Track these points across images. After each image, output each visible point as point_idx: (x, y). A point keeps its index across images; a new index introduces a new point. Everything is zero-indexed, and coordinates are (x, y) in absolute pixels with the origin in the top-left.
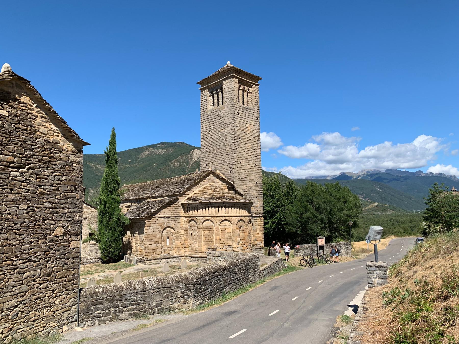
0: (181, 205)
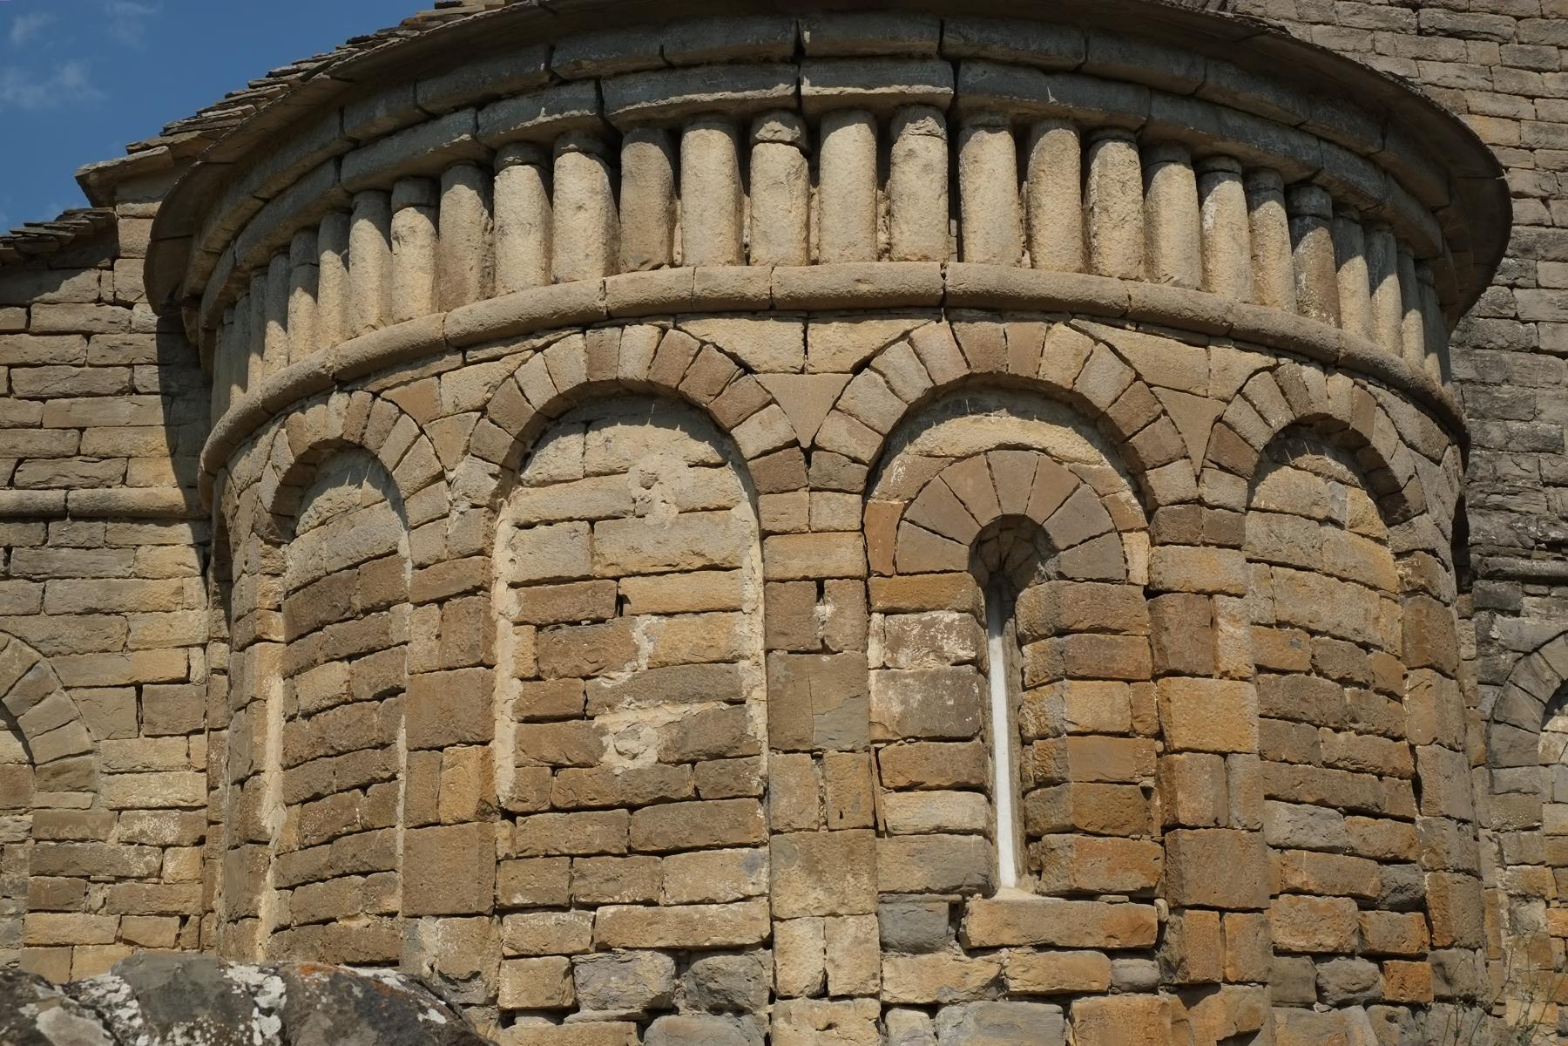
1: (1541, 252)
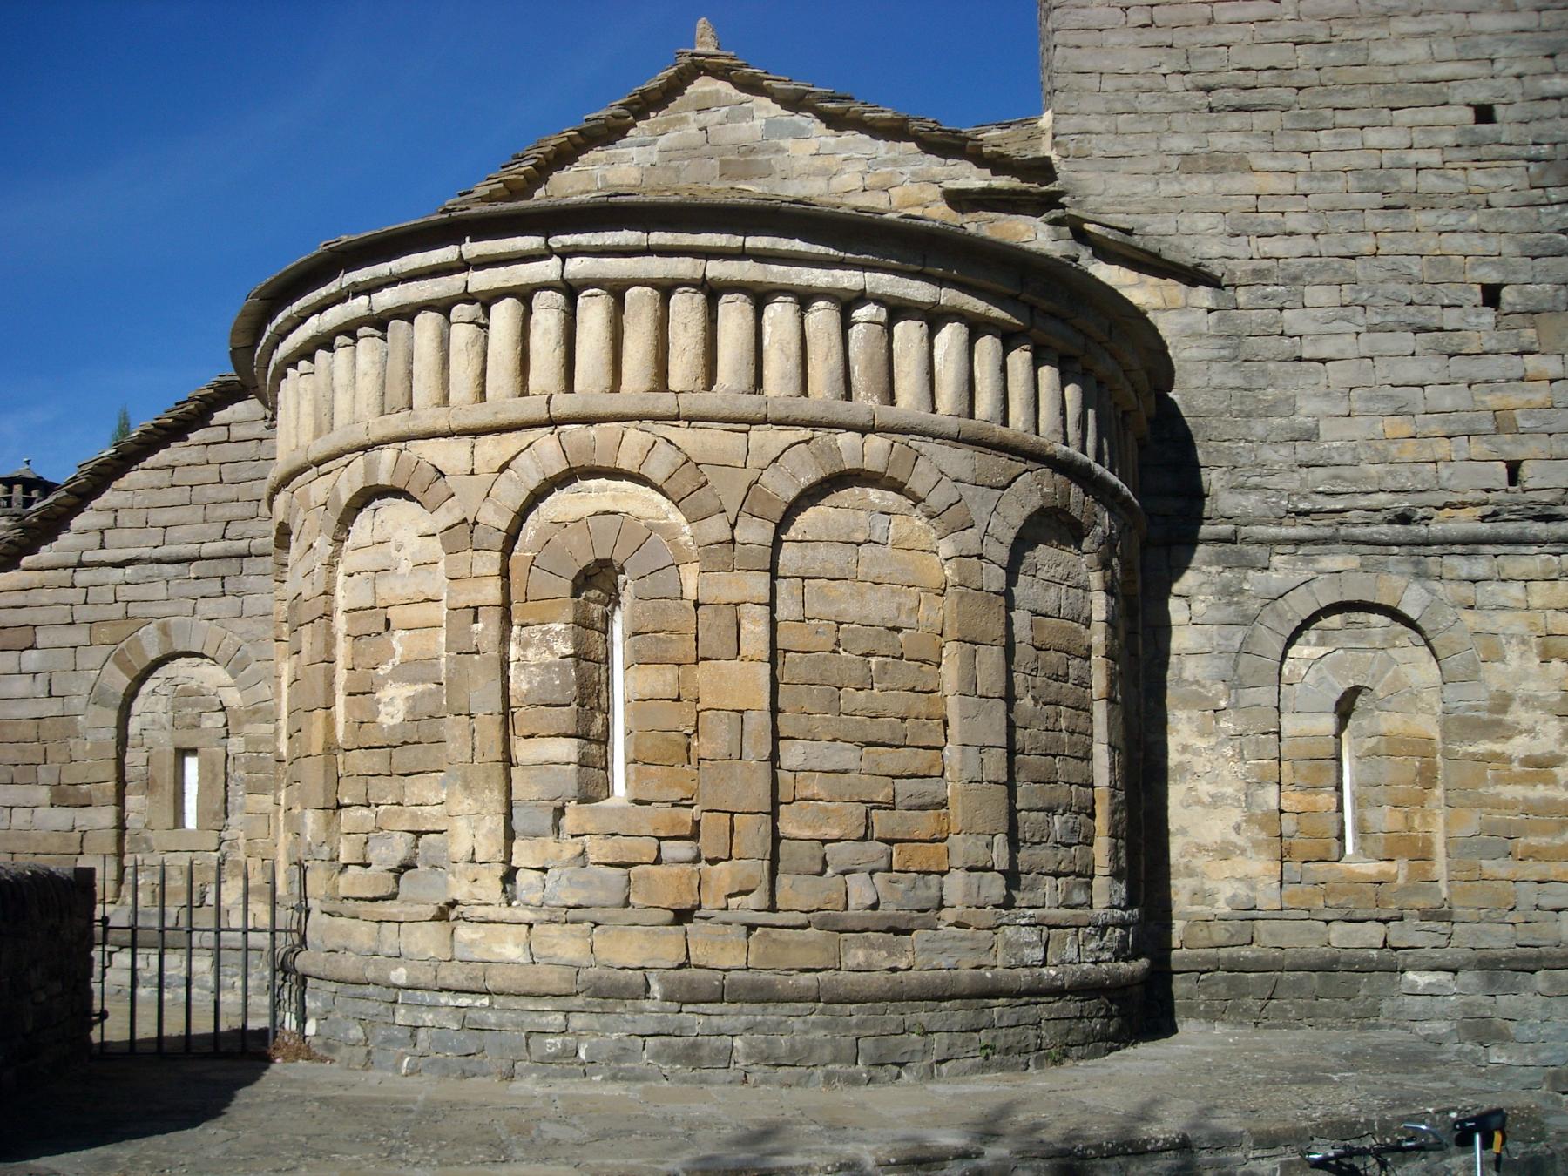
1: (1308, 278)
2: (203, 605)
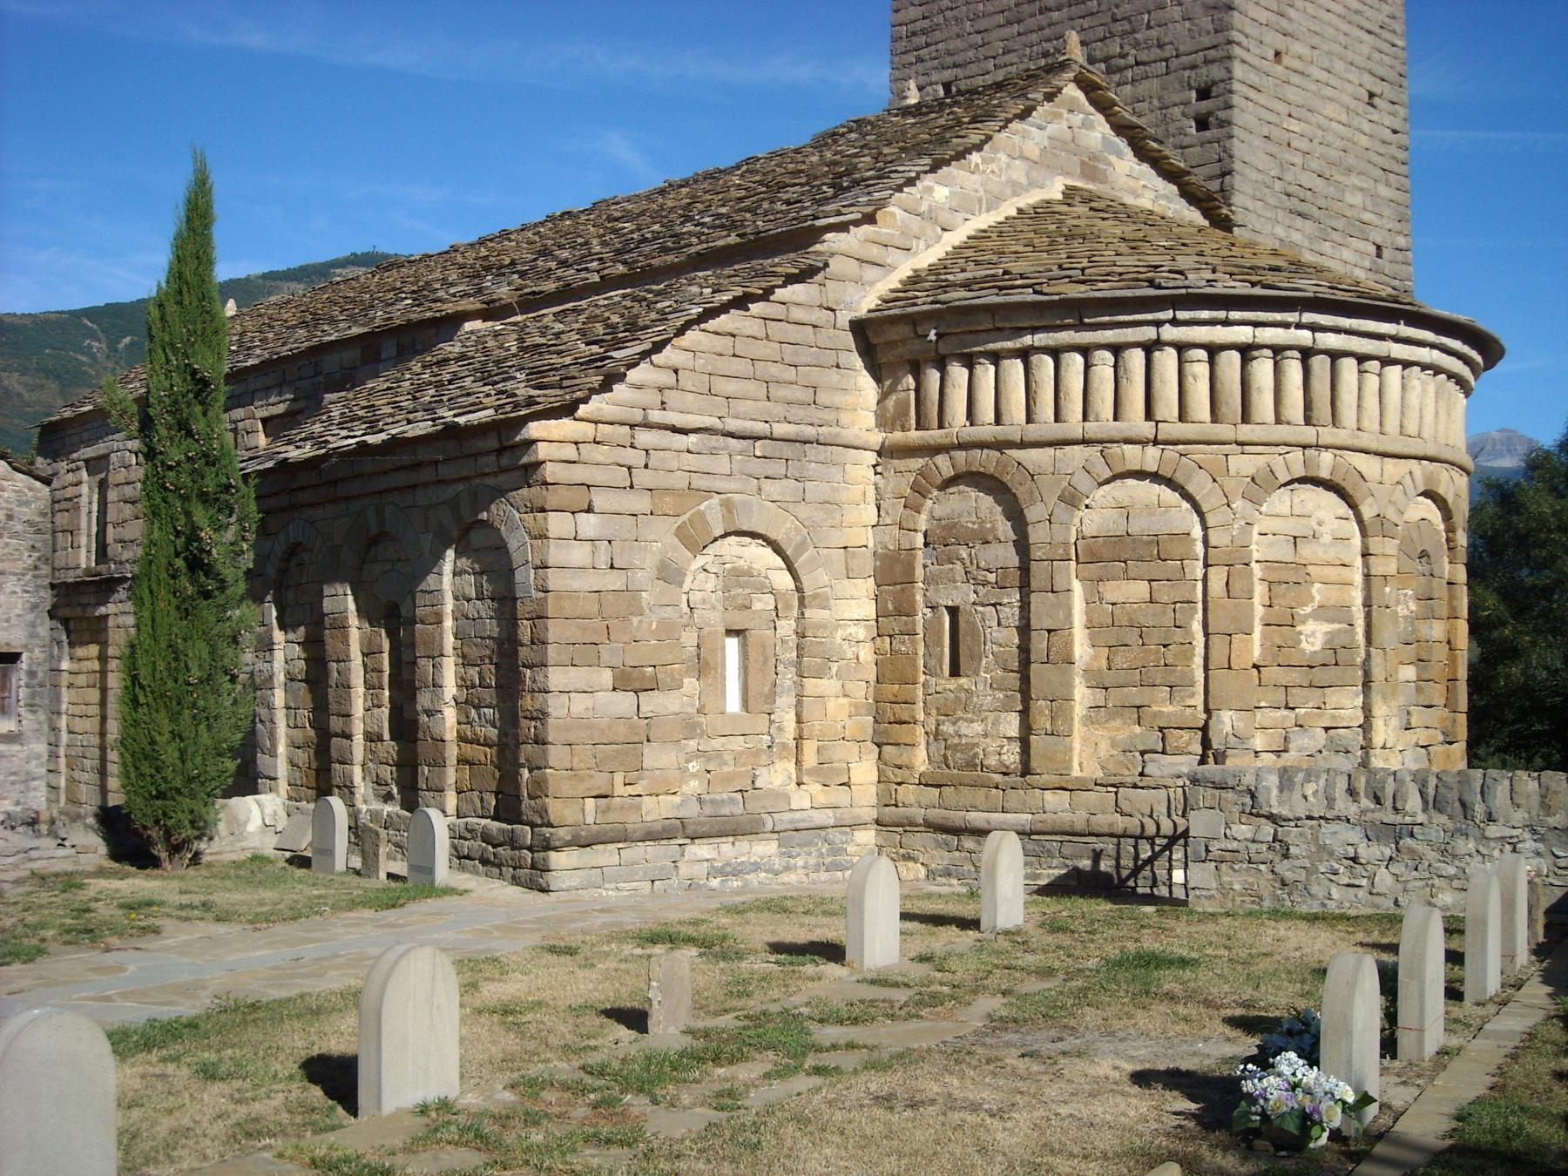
0: (848, 340)
2: (767, 485)
